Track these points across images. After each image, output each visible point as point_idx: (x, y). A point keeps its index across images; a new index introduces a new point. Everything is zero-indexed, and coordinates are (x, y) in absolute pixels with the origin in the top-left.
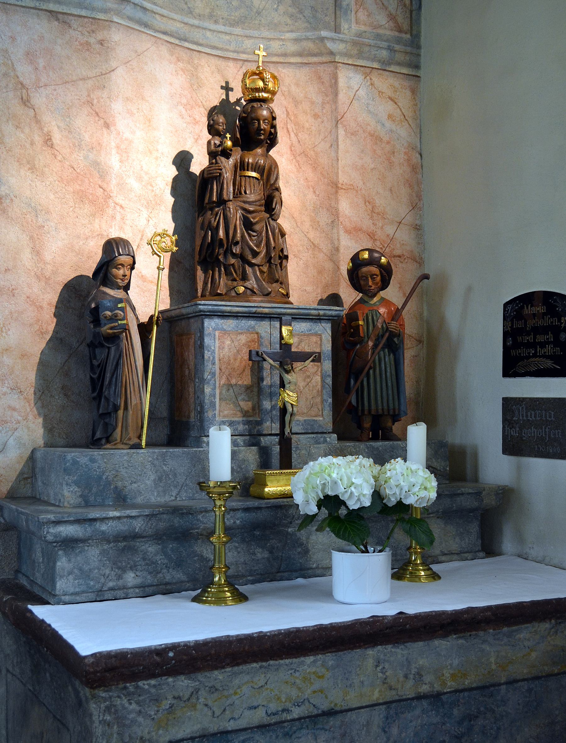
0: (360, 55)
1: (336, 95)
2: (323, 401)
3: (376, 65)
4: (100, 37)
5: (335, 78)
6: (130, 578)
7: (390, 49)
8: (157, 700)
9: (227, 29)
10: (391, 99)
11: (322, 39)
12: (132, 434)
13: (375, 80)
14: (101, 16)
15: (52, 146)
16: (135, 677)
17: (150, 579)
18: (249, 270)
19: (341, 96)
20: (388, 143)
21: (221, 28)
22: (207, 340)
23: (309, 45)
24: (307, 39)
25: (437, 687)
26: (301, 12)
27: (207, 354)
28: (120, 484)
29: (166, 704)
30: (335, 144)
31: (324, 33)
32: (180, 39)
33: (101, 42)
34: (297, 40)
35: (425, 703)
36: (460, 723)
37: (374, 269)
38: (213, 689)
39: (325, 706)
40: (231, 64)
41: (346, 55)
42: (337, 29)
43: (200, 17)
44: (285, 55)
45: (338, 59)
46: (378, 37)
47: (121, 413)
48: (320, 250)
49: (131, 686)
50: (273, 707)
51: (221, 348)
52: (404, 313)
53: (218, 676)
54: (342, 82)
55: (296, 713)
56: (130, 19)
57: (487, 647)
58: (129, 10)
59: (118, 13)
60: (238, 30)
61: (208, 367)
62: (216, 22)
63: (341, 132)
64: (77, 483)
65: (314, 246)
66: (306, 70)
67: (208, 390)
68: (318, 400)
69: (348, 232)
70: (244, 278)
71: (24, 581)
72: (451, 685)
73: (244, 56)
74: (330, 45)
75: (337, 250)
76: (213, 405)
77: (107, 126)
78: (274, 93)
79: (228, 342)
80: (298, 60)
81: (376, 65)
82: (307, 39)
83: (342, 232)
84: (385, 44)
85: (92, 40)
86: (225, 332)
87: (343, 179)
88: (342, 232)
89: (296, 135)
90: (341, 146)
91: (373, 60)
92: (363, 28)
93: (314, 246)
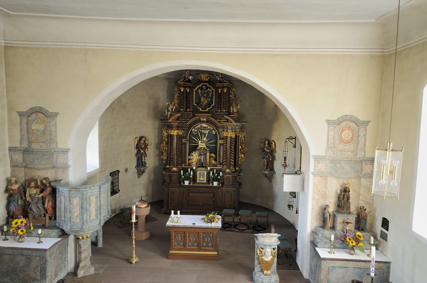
0: (365, 176)
1: (360, 182)
2: (353, 227)
3: (367, 177)
4: (326, 178)
5: (361, 180)
6: (326, 246)
7: (370, 175)
8: (328, 262)
9: (344, 175)
10: (370, 182)
11: (359, 175)
12: (328, 228)
13: (367, 179)
14: (327, 176)
15: (320, 192)
16: (326, 260)
17: (329, 246)
18: (344, 209)
19: (361, 182)
20: (369, 188)
21: (343, 175)
22: (338, 219)
23: (357, 176)
24: (357, 175)
25: (360, 267)
26: (356, 171)
27: (337, 221)
28: (326, 235)
29: (329, 263)
30: (360, 189)
31: (359, 174)
32: (337, 177)
33: (327, 179)
34: (355, 175)
35: (359, 268)
36: (363, 271)
37: (363, 209)
38: (334, 262)
39: (346, 266)
40: (344, 179)
41: (363, 176)
42: (361, 173)
43: (340, 174)
44: (353, 177)
45: (361, 177)
46: (368, 173)
47: (326, 226)
48: (356, 203)
49: (325, 261)
50: (340, 265)
51: (339, 220)
52: (368, 215)
53: (334, 261)
54: (362, 180)
55: (343, 266)
56: (330, 175)
57: (367, 264)
58: (330, 174)
59: (329, 175)
60: (345, 175)
61: (338, 222)
62: (343, 174)
63: (361, 187)
64: (321, 234)
65: (355, 203)
66: (356, 179)
67: (337, 225)
68: (352, 227)
69: (361, 201)
70: (343, 210)
71: (314, 241)
72: (362, 267)
73: (346, 178)
74: (360, 175)
75: (359, 203)
76: (338, 227)
77: (327, 189)
78: (349, 187)
79: (340, 219)
80: (355, 178)
81: (367, 177)
82: (357, 175)
83: (360, 201)
84: (369, 174)
85: (325, 179)
86: (340, 218)
87: (361, 193)
88: (360, 201)
89: (354, 188)
90: (361, 189)
91: (367, 176)
92: (365, 172)
93: (355, 203)
